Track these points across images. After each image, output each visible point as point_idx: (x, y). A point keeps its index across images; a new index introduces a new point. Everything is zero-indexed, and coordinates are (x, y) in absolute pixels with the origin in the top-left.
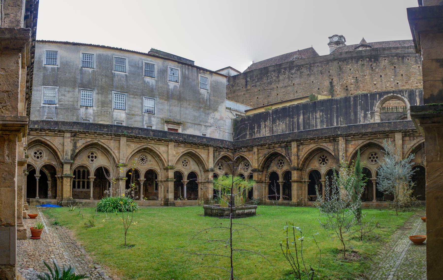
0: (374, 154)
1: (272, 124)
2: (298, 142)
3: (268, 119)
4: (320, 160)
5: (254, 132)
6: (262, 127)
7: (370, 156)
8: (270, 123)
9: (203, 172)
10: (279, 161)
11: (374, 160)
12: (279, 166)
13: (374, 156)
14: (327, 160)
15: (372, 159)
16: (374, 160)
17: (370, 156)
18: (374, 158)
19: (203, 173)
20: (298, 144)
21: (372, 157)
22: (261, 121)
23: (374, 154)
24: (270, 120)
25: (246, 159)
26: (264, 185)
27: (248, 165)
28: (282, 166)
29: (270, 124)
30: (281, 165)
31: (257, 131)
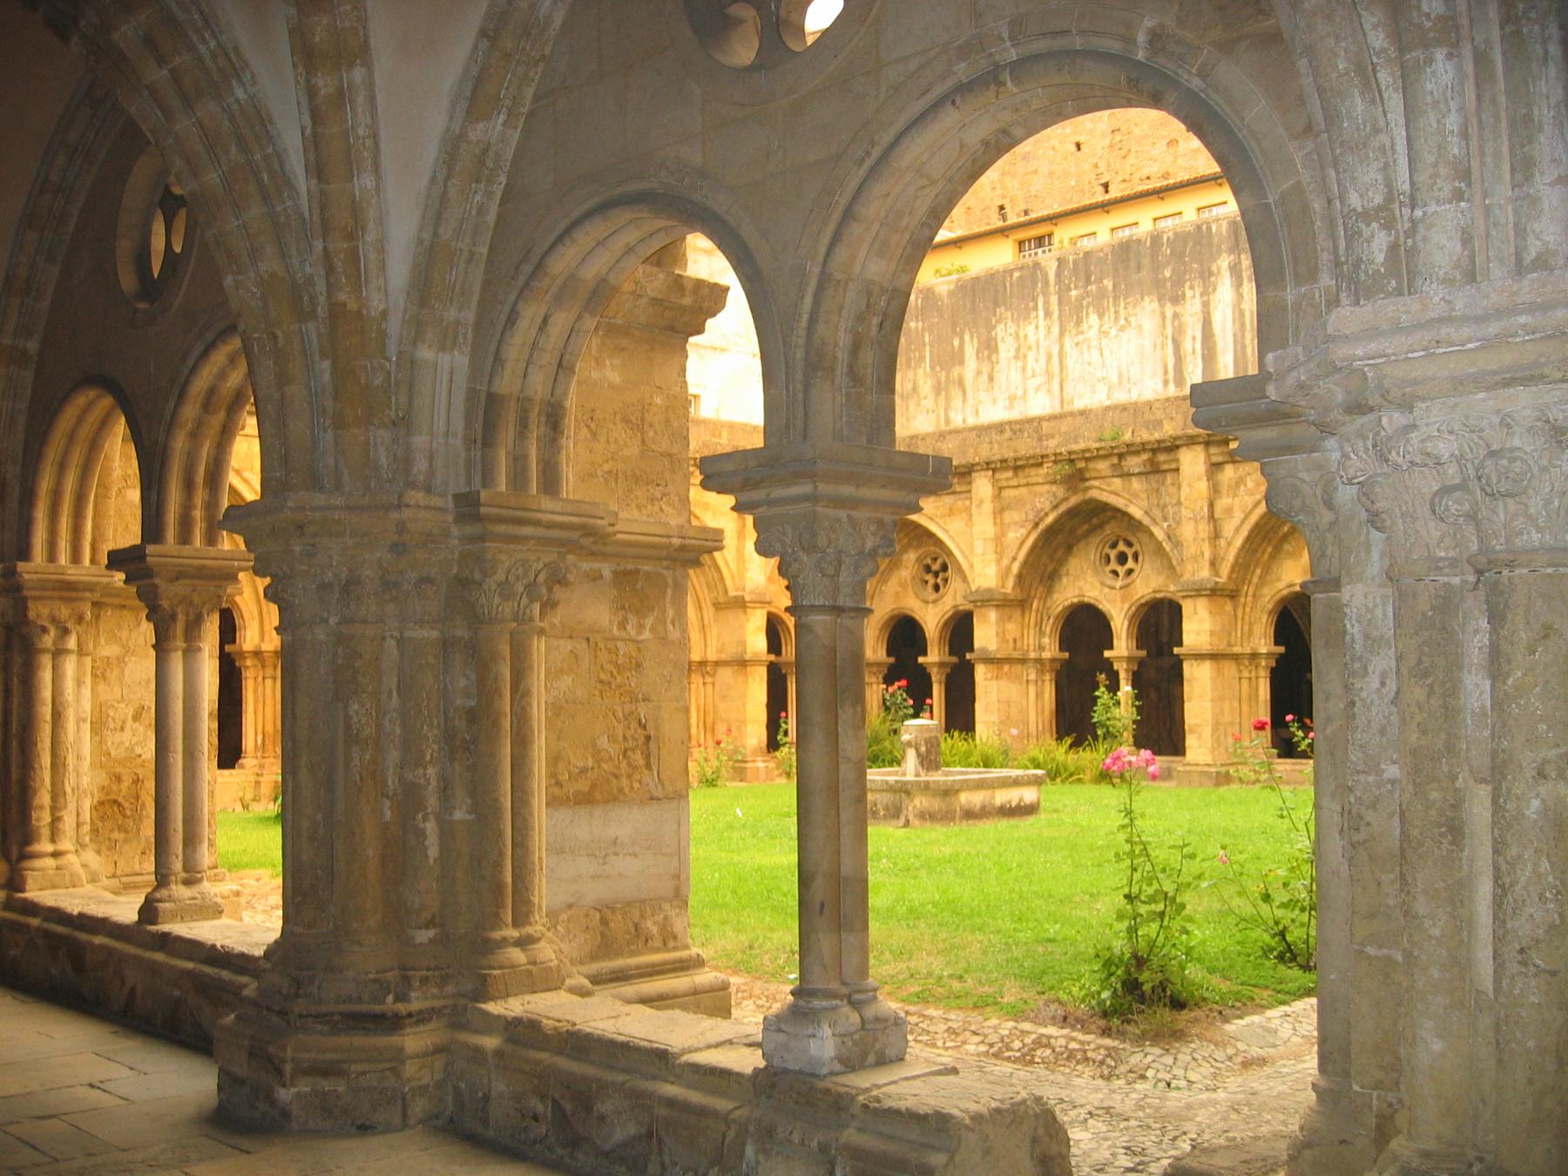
2: (1213, 450)
3: (1035, 308)
5: (961, 383)
8: (1049, 330)
9: (712, 609)
10: (1114, 546)
12: (1115, 573)
19: (709, 612)
20: (1215, 459)
22: (999, 321)
24: (1048, 314)
25: (931, 535)
27: (944, 568)
28: (1130, 572)
30: (1121, 570)
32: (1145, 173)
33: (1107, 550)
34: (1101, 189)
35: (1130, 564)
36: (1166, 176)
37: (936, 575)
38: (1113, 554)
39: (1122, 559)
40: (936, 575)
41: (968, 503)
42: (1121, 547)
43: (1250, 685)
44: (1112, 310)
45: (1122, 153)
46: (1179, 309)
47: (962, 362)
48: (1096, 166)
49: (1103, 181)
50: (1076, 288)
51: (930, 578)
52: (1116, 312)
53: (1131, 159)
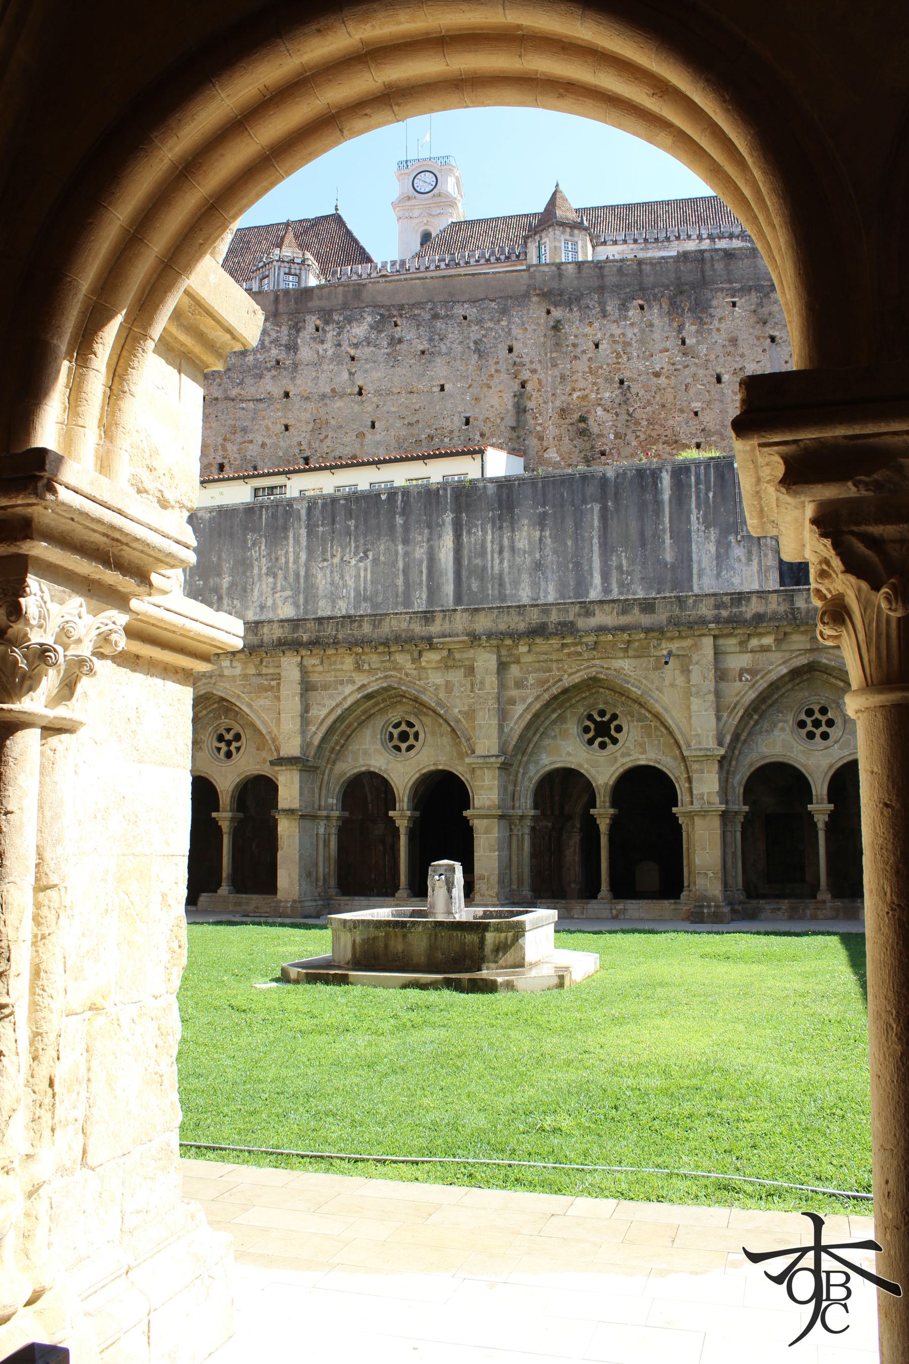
0: (816, 708)
1: (309, 559)
4: (586, 730)
6: (256, 571)
7: (803, 717)
11: (818, 732)
13: (817, 715)
14: (619, 729)
15: (810, 727)
16: (818, 732)
17: (803, 717)
18: (817, 724)
21: (809, 721)
23: (816, 708)
26: (322, 830)
27: (238, 737)
29: (296, 561)
31: (232, 585)
32: (337, 454)
33: (391, 729)
34: (301, 461)
35: (411, 741)
36: (354, 457)
37: (229, 743)
38: (396, 732)
39: (404, 737)
40: (229, 743)
41: (274, 683)
42: (404, 727)
43: (518, 841)
44: (353, 545)
45: (322, 437)
46: (409, 549)
47: (219, 575)
48: (300, 444)
49: (305, 455)
50: (322, 525)
51: (223, 745)
52: (357, 547)
53: (328, 442)
